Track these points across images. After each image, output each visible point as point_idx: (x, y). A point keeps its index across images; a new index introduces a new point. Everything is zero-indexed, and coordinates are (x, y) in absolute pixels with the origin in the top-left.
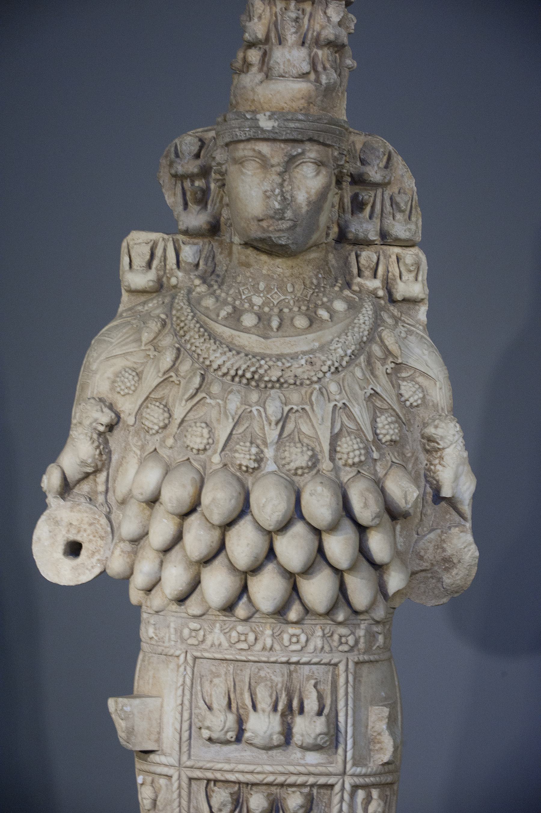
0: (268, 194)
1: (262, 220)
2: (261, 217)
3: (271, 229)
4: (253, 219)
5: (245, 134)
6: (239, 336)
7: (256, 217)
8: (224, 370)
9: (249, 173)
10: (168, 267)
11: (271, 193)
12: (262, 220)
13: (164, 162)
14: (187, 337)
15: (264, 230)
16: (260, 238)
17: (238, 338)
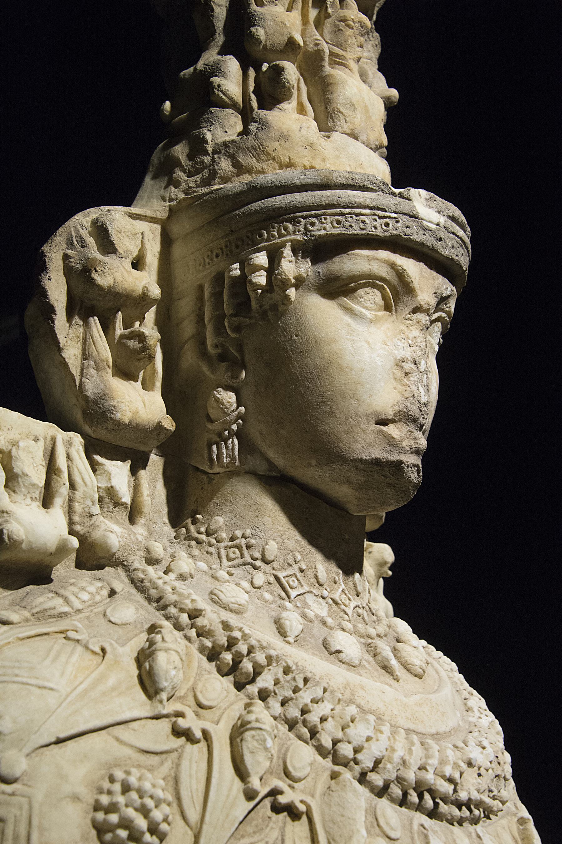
0: (408, 366)
1: (384, 422)
2: (390, 413)
3: (404, 444)
4: (367, 416)
5: (387, 225)
6: (362, 688)
7: (377, 414)
8: (390, 771)
9: (368, 314)
10: (78, 507)
11: (413, 366)
12: (384, 422)
13: (55, 253)
14: (265, 681)
15: (392, 443)
16: (376, 462)
17: (361, 692)
